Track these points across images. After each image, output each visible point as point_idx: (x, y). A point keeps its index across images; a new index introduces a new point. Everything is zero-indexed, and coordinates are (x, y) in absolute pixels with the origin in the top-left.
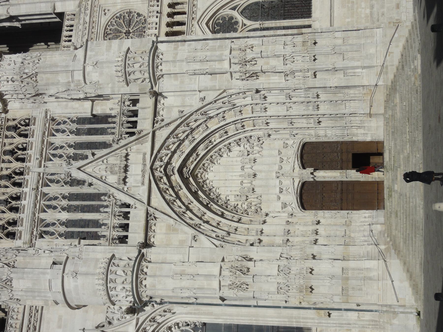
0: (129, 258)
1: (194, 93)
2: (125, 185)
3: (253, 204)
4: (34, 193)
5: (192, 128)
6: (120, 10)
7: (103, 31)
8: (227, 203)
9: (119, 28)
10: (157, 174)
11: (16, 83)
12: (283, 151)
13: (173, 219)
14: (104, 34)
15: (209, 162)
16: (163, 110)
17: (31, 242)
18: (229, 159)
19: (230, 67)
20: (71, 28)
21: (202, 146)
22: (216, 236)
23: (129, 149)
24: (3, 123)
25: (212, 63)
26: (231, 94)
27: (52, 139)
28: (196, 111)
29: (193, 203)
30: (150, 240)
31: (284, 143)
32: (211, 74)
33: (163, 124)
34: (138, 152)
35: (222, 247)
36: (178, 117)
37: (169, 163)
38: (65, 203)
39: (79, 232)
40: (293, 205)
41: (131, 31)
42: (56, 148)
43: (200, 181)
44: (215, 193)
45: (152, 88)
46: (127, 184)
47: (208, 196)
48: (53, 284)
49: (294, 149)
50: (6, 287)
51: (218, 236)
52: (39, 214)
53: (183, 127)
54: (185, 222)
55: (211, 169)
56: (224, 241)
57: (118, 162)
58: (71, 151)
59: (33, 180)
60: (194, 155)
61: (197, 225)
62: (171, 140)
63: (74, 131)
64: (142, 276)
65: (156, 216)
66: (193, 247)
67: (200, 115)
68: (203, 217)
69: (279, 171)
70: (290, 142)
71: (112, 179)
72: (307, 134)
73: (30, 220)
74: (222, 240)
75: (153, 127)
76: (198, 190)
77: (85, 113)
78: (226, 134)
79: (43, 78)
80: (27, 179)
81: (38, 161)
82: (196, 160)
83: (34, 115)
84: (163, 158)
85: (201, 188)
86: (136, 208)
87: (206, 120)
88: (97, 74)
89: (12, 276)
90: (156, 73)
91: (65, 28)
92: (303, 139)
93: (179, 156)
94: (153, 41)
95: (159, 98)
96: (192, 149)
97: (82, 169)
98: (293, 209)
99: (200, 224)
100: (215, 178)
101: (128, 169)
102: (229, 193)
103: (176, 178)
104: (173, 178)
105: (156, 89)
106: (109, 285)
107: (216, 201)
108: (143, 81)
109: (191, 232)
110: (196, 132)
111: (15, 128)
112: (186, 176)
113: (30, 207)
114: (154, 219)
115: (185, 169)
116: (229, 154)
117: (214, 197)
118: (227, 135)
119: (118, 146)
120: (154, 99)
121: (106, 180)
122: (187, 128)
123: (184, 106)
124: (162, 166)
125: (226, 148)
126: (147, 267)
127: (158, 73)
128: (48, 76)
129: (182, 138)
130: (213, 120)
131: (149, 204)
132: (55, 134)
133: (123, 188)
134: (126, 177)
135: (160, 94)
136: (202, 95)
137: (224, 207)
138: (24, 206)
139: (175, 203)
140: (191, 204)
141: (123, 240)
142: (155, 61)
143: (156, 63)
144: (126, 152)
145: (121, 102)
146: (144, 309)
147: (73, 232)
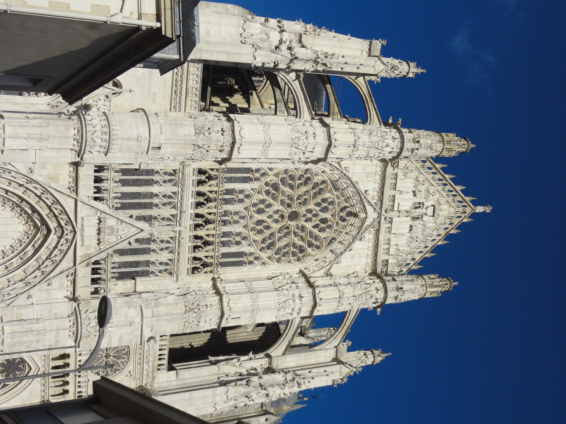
0: (92, 153)
1: (39, 303)
2: (99, 217)
4: (183, 209)
5: (39, 270)
6: (116, 376)
7: (131, 356)
8: (4, 204)
9: (116, 360)
10: (70, 228)
11: (204, 304)
13: (52, 188)
14: (129, 354)
15: (23, 241)
16: (68, 286)
17: (183, 166)
19: (3, 327)
20: (160, 357)
21: (30, 254)
22: (11, 173)
23: (98, 249)
24: (216, 269)
25: (22, 330)
26: (2, 303)
27: (171, 256)
28: (35, 285)
29: (36, 203)
30: (74, 169)
32: (22, 320)
33: (66, 273)
34: (89, 247)
35: (4, 163)
36: (52, 280)
37: (60, 238)
38: (156, 201)
39: (142, 175)
41: (104, 358)
42: (167, 248)
43: (31, 223)
44: (16, 212)
45: (78, 305)
46: (97, 218)
47: (22, 209)
48: (159, 131)
50: (200, 128)
51: (9, 173)
52: (178, 191)
53: (47, 270)
54: (41, 185)
55: (21, 234)
56: (3, 168)
57: (107, 237)
58: (153, 246)
59: (185, 220)
60: (36, 246)
61: (30, 183)
62: (58, 258)
63: (152, 264)
64: (78, 137)
65: (69, 190)
66: (33, 163)
67: (32, 282)
68: (25, 190)
71: (111, 222)
73: (186, 185)
74: (5, 169)
75: (75, 269)
76: (32, 214)
77: (142, 281)
78: (7, 266)
79: (180, 309)
80: (191, 220)
81: (182, 236)
82: (35, 242)
83: (188, 277)
84: (65, 242)
85: (29, 217)
86: (88, 197)
87: (26, 278)
88: (130, 315)
89: (195, 138)
90: (74, 319)
91: (166, 357)
93: (50, 244)
94: (79, 347)
95: (71, 296)
96: (39, 251)
97: (140, 230)
99: (27, 183)
100: (17, 225)
101: (98, 232)
103: (53, 225)
104: (56, 225)
105: (75, 304)
106: (108, 129)
107: (15, 204)
108: (87, 310)
109: (35, 177)
110: (35, 267)
111: (205, 265)
112: (43, 226)
113: (187, 196)
114: (71, 187)
115: (45, 233)
116: (4, 248)
117: (16, 209)
118: (5, 266)
119: (107, 251)
120: (76, 295)
121: (117, 221)
122: (44, 270)
123: (48, 290)
124: (66, 235)
125: (7, 254)
126: (74, 145)
127: (73, 318)
128: (175, 312)
129: (48, 261)
130: (20, 279)
131: (76, 200)
132: (169, 262)
133: (101, 214)
134: (99, 224)
135: (70, 300)
136: (30, 301)
137: (6, 200)
138: (192, 198)
139: (52, 202)
140: (37, 202)
141: (100, 169)
142: (76, 329)
143: (75, 328)
144: (100, 246)
145: (107, 291)
146: (76, 109)
147: (147, 175)
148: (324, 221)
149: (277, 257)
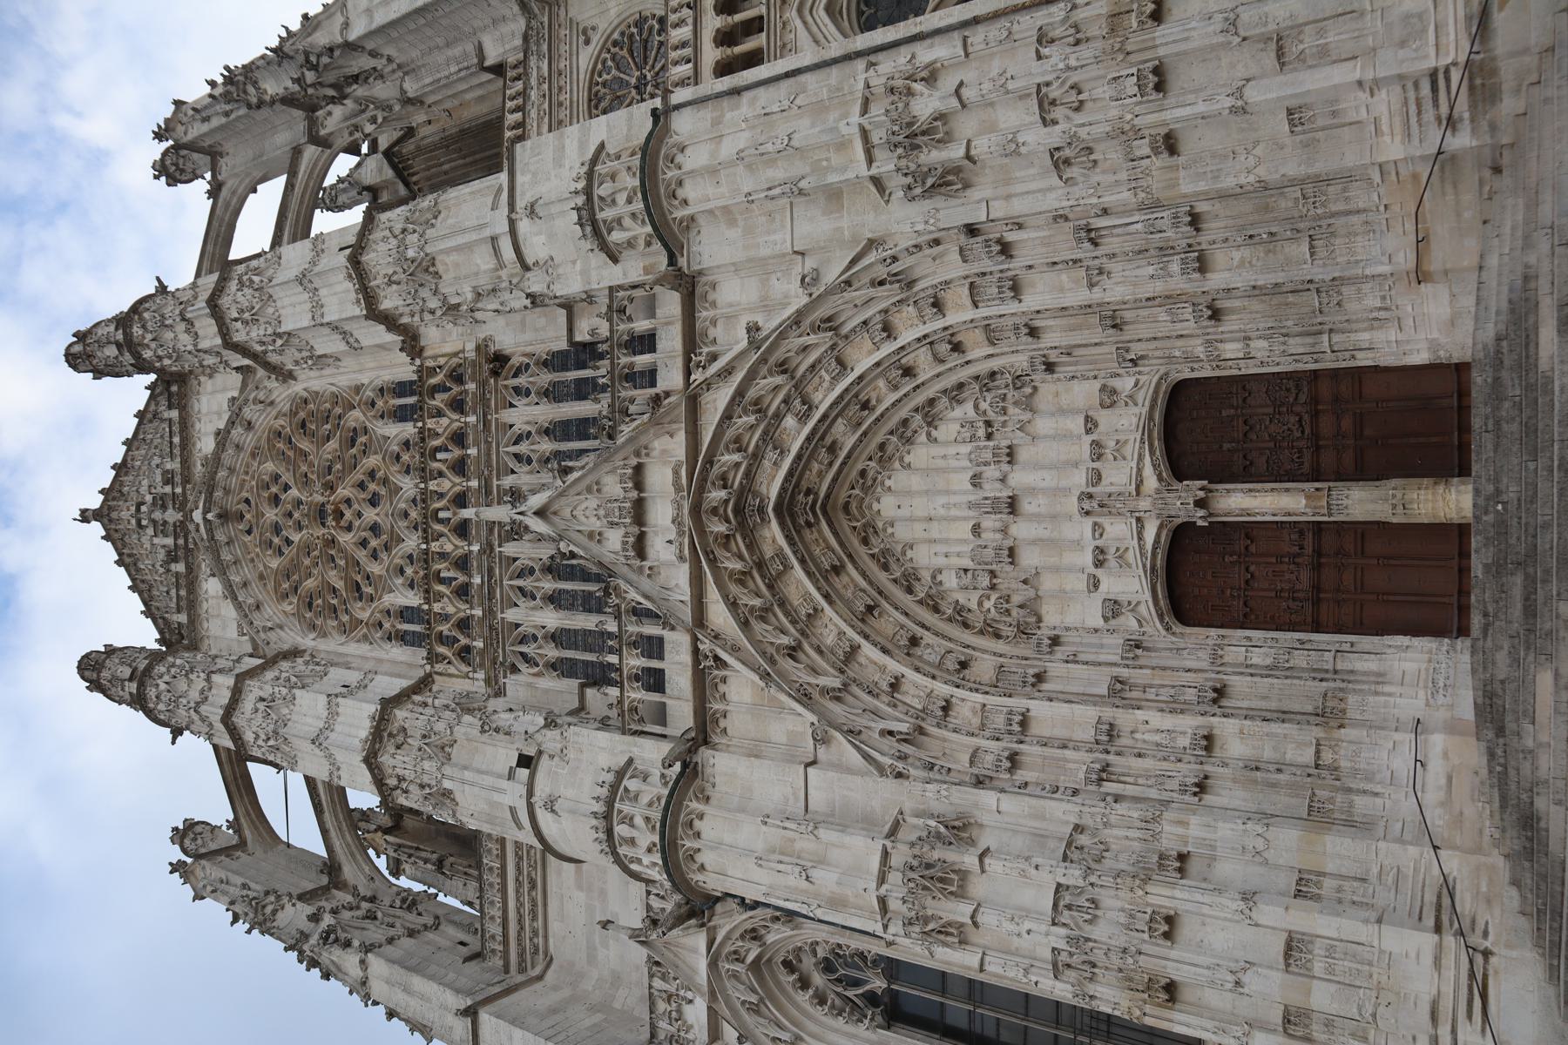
3: (1017, 599)
6: (616, 23)
12: (1105, 418)
18: (936, 450)
21: (840, 426)
31: (1103, 388)
40: (1143, 609)
49: (1136, 410)
69: (1091, 490)
70: (1125, 384)
71: (615, 539)
72: (1177, 354)
82: (831, 464)
88: (542, 238)
89: (447, 784)
90: (671, 213)
92: (1167, 374)
93: (775, 463)
98: (1144, 623)
100: (900, 513)
102: (940, 561)
148: (275, 500)
149: (338, 410)
